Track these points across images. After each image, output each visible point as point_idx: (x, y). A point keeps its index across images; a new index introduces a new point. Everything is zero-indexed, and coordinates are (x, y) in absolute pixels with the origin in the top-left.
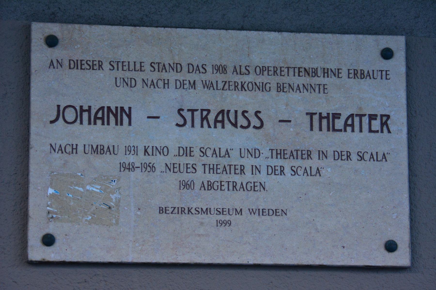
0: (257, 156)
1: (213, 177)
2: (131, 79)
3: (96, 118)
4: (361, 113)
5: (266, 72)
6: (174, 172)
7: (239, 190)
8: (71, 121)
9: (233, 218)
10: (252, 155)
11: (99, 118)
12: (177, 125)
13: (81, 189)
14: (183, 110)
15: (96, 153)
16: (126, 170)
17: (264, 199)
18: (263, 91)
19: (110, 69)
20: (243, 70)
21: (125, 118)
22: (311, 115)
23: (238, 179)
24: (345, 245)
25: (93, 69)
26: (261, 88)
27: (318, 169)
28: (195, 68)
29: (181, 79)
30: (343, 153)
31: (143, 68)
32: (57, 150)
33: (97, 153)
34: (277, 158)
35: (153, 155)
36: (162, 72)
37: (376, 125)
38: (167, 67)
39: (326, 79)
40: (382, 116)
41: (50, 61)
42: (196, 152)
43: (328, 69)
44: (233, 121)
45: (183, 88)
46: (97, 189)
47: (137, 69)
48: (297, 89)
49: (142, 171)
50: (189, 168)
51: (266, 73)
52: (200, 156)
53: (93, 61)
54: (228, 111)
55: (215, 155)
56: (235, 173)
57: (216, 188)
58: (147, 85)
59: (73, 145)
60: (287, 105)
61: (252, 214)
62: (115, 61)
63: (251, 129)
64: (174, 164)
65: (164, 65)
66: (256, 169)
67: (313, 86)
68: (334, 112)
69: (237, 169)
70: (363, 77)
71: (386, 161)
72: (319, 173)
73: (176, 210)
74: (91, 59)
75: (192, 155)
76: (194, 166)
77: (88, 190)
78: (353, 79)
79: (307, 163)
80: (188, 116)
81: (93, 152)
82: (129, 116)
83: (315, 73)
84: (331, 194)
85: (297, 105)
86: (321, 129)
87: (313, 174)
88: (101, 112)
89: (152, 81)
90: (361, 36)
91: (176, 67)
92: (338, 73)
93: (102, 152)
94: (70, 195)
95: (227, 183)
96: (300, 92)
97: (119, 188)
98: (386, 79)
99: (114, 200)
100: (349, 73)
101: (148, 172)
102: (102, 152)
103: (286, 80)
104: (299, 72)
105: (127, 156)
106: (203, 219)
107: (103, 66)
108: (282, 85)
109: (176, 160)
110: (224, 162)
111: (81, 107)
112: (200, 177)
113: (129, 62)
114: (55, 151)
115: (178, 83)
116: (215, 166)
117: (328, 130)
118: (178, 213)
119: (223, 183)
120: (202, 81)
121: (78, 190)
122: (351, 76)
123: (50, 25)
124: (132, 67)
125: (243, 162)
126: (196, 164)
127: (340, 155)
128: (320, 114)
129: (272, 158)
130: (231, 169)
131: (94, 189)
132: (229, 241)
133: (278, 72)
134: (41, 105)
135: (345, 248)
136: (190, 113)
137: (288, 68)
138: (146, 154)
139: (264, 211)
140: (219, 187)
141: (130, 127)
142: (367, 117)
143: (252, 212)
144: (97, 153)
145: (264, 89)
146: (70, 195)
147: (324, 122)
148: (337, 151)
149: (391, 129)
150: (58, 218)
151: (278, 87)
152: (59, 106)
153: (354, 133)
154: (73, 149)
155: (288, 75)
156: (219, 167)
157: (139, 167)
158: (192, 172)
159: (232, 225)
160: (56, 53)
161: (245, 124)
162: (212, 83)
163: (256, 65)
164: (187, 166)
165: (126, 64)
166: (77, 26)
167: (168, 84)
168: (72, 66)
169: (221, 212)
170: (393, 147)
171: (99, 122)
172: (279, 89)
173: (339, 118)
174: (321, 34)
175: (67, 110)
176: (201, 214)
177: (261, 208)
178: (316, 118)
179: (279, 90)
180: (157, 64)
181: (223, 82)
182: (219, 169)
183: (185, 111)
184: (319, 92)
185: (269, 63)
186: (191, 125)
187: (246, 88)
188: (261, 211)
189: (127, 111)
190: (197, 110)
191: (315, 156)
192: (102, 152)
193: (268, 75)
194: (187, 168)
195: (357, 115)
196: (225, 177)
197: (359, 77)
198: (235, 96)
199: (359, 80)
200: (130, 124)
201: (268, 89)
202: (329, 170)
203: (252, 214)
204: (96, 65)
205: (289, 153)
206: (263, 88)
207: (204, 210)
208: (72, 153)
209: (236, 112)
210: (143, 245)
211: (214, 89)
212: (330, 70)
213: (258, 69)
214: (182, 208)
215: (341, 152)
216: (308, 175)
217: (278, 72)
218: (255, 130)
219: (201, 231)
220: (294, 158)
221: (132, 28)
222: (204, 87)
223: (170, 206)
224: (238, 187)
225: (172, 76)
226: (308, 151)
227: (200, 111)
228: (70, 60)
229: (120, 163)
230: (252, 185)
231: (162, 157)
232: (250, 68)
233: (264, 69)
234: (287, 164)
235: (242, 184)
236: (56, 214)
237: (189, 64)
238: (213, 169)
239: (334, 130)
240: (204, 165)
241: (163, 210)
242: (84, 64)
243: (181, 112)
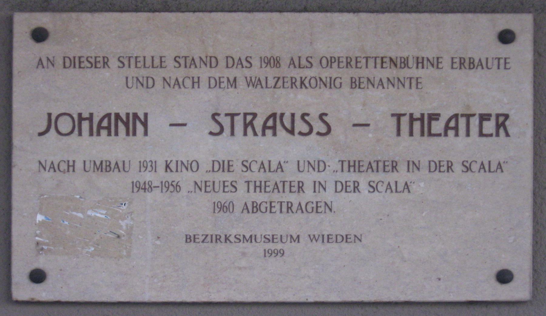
1: (260, 197)
3: (100, 127)
9: (288, 247)
10: (314, 169)
11: (104, 128)
12: (211, 133)
14: (218, 115)
18: (330, 88)
20: (304, 62)
22: (399, 117)
23: (294, 198)
26: (328, 85)
27: (406, 184)
31: (163, 64)
32: (47, 168)
34: (349, 171)
35: (177, 171)
37: (489, 126)
38: (197, 61)
40: (498, 116)
42: (237, 166)
51: (335, 65)
54: (282, 115)
57: (263, 209)
58: (169, 85)
60: (364, 105)
63: (313, 136)
65: (193, 59)
76: (234, 184)
77: (89, 216)
79: (391, 177)
80: (226, 122)
82: (145, 124)
83: (405, 63)
85: (379, 104)
91: (211, 61)
92: (438, 63)
97: (131, 213)
100: (453, 63)
109: (210, 177)
111: (80, 115)
112: (242, 196)
115: (213, 81)
116: (263, 184)
117: (422, 134)
129: (342, 171)
132: (281, 275)
133: (353, 63)
137: (367, 58)
142: (477, 117)
143: (313, 238)
154: (69, 166)
156: (268, 184)
171: (104, 132)
173: (437, 119)
177: (326, 233)
178: (405, 121)
183: (222, 116)
184: (410, 87)
185: (339, 51)
186: (230, 134)
187: (307, 85)
189: (142, 117)
190: (238, 114)
191: (402, 168)
193: (339, 67)
194: (224, 186)
195: (462, 115)
196: (276, 197)
197: (467, 67)
199: (467, 71)
200: (146, 133)
205: (366, 165)
206: (331, 84)
207: (248, 237)
209: (293, 115)
212: (425, 60)
213: (324, 61)
217: (353, 63)
218: (318, 137)
219: (243, 263)
224: (294, 208)
225: (204, 73)
227: (242, 116)
230: (314, 205)
234: (363, 180)
235: (300, 204)
238: (260, 187)
239: (430, 134)
241: (189, 239)
243: (216, 117)
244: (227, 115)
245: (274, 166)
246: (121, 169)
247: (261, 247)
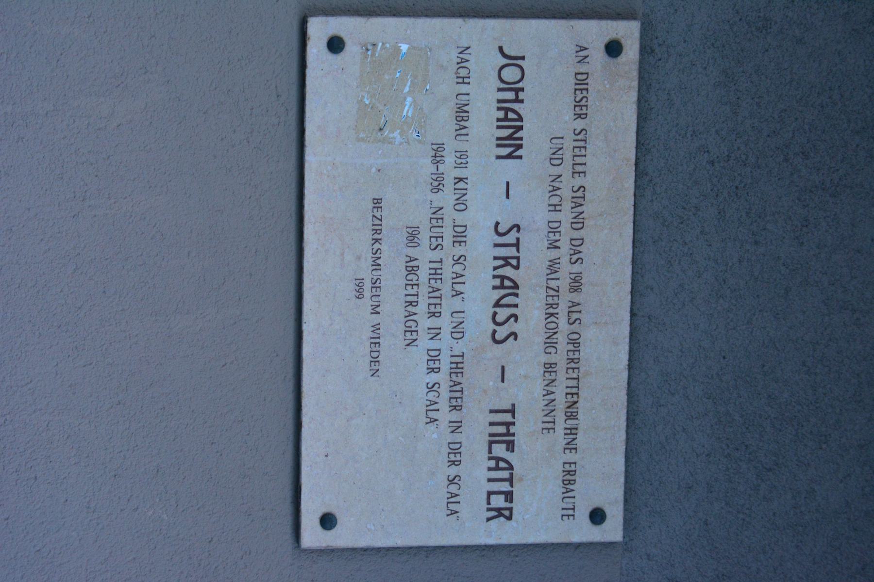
0: (455, 335)
1: (424, 274)
3: (507, 110)
4: (514, 481)
9: (367, 303)
10: (455, 327)
11: (506, 114)
12: (497, 224)
13: (407, 89)
14: (518, 231)
18: (546, 343)
20: (575, 316)
22: (512, 411)
23: (422, 308)
24: (329, 458)
25: (575, 106)
26: (549, 341)
27: (436, 420)
31: (576, 175)
32: (461, 56)
34: (451, 363)
35: (455, 189)
37: (498, 501)
38: (580, 209)
39: (563, 432)
40: (510, 510)
41: (586, 46)
42: (459, 250)
44: (503, 302)
51: (571, 347)
53: (586, 106)
54: (517, 295)
55: (455, 276)
56: (429, 304)
57: (409, 277)
58: (553, 181)
60: (526, 377)
63: (493, 326)
65: (581, 205)
67: (552, 414)
74: (589, 103)
76: (440, 247)
77: (405, 99)
79: (444, 405)
80: (511, 238)
82: (509, 156)
83: (571, 415)
85: (526, 392)
86: (491, 424)
87: (429, 413)
88: (515, 117)
89: (559, 189)
90: (622, 480)
91: (578, 222)
92: (571, 449)
97: (408, 143)
98: (563, 516)
99: (391, 135)
100: (570, 463)
104: (572, 394)
109: (448, 222)
111: (522, 90)
112: (425, 256)
113: (585, 156)
115: (556, 225)
116: (440, 277)
117: (491, 435)
121: (405, 85)
122: (567, 466)
123: (636, 47)
124: (578, 160)
127: (456, 452)
128: (513, 424)
129: (452, 356)
132: (335, 295)
133: (573, 365)
134: (527, 34)
137: (578, 379)
140: (410, 282)
142: (510, 489)
143: (376, 328)
147: (502, 429)
150: (366, 58)
152: (523, 58)
154: (463, 78)
156: (439, 281)
160: (598, 54)
161: (500, 318)
162: (557, 272)
165: (583, 152)
166: (635, 84)
168: (579, 77)
170: (467, 524)
171: (501, 114)
173: (508, 450)
174: (625, 424)
175: (517, 71)
177: (381, 341)
178: (508, 417)
183: (517, 235)
184: (543, 422)
185: (585, 352)
186: (497, 242)
187: (549, 320)
188: (377, 341)
189: (517, 153)
190: (518, 251)
191: (455, 416)
193: (568, 351)
194: (437, 237)
195: (512, 474)
196: (424, 290)
197: (565, 478)
198: (538, 304)
199: (561, 479)
200: (498, 157)
202: (435, 436)
205: (458, 380)
206: (550, 343)
207: (378, 262)
208: (458, 77)
209: (516, 306)
212: (574, 436)
213: (576, 336)
217: (573, 365)
218: (491, 331)
219: (348, 257)
220: (451, 387)
221: (634, 161)
224: (410, 308)
225: (566, 216)
227: (516, 254)
228: (587, 74)
230: (413, 329)
234: (442, 378)
235: (415, 314)
236: (372, 56)
238: (436, 274)
239: (491, 443)
241: (377, 203)
243: (515, 229)
244: (518, 239)
245: (458, 287)
246: (458, 132)
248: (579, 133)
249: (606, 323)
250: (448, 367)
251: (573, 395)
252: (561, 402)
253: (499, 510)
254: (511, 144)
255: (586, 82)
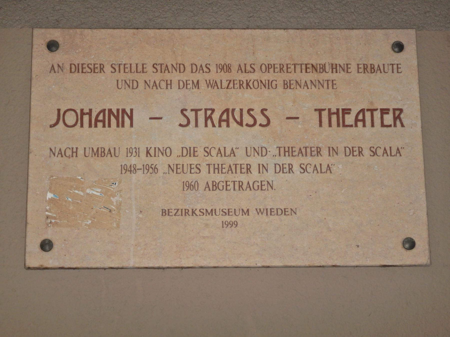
0: (264, 153)
1: (218, 177)
2: (133, 81)
3: (97, 120)
4: (372, 108)
5: (272, 69)
6: (177, 173)
7: (246, 190)
8: (72, 125)
9: (240, 218)
10: (258, 154)
11: (100, 121)
12: (181, 125)
13: (82, 194)
14: (186, 110)
15: (96, 155)
16: (127, 172)
17: (272, 198)
18: (269, 88)
19: (112, 72)
20: (248, 68)
21: (127, 120)
22: (320, 111)
23: (244, 178)
24: (359, 244)
25: (94, 72)
26: (267, 86)
27: (328, 166)
28: (199, 67)
29: (185, 79)
30: (355, 149)
31: (145, 70)
32: (56, 154)
33: (98, 156)
34: (285, 155)
35: (155, 156)
36: (164, 72)
37: (389, 119)
38: (170, 67)
39: (335, 74)
40: (394, 110)
41: (50, 66)
42: (201, 152)
43: (336, 65)
44: (238, 119)
45: (187, 88)
46: (98, 192)
47: (139, 71)
48: (304, 86)
49: (144, 173)
50: (193, 168)
51: (271, 70)
52: (205, 156)
53: (94, 64)
54: (233, 110)
55: (219, 155)
56: (241, 173)
57: (221, 188)
58: (149, 87)
59: (73, 148)
60: (294, 102)
61: (260, 214)
62: (116, 63)
63: (257, 127)
64: (177, 165)
65: (167, 66)
66: (263, 168)
67: (322, 82)
68: (344, 108)
69: (244, 168)
70: (373, 71)
71: (401, 155)
72: (330, 170)
73: (179, 212)
74: (93, 62)
75: (195, 155)
76: (198, 166)
77: (88, 194)
78: (362, 74)
79: (316, 160)
80: (191, 115)
81: (93, 155)
82: (131, 118)
83: (323, 68)
84: (343, 192)
85: (305, 102)
86: (330, 125)
87: (323, 171)
88: (102, 115)
89: (155, 82)
90: (369, 31)
91: (180, 68)
92: (347, 68)
93: (103, 154)
94: (70, 199)
95: (233, 182)
96: (308, 88)
97: (121, 191)
98: (398, 72)
99: (115, 204)
100: (358, 68)
101: (151, 173)
102: (103, 155)
103: (293, 76)
104: (306, 68)
105: (129, 158)
106: (208, 220)
107: (104, 69)
108: (288, 81)
109: (180, 161)
110: (230, 161)
111: (82, 110)
112: (204, 178)
113: (131, 64)
114: (54, 155)
115: (181, 84)
116: (220, 166)
117: (338, 125)
118: (182, 215)
119: (228, 183)
120: (206, 81)
121: (78, 194)
122: (361, 70)
123: (52, 31)
124: (134, 69)
125: (249, 160)
126: (200, 165)
127: (352, 151)
128: (329, 110)
129: (280, 155)
130: (237, 168)
131: (95, 193)
132: (235, 243)
133: (285, 68)
134: (42, 109)
135: (360, 247)
136: (194, 113)
137: (295, 65)
138: (148, 155)
139: (272, 210)
140: (225, 187)
141: (132, 129)
142: (379, 111)
143: (259, 211)
144: (98, 156)
145: (270, 87)
146: (70, 199)
147: (334, 118)
148: (348, 147)
149: (405, 123)
150: (56, 223)
151: (284, 84)
152: (59, 110)
153: (365, 128)
154: (73, 152)
155: (295, 72)
156: (224, 166)
157: (141, 169)
158: (196, 173)
159: (238, 225)
160: (58, 57)
161: (251, 122)
162: (216, 82)
163: (261, 63)
164: (177, 167)
165: (128, 66)
166: (78, 31)
167: (171, 84)
168: (73, 70)
169: (227, 213)
170: (407, 141)
171: (100, 125)
172: (286, 86)
173: (349, 113)
174: (328, 31)
175: (68, 114)
176: (206, 215)
177: (269, 208)
178: (325, 114)
179: (286, 87)
180: (160, 65)
181: (227, 81)
182: (225, 168)
183: (189, 111)
184: (328, 88)
185: (275, 60)
186: (194, 125)
187: (252, 86)
188: (269, 210)
189: (129, 112)
190: (200, 110)
191: (325, 152)
192: (103, 154)
193: (274, 72)
194: (191, 168)
195: (368, 110)
196: (231, 177)
197: (370, 71)
198: (240, 94)
199: (370, 74)
200: (132, 125)
201: (274, 86)
202: (340, 166)
203: (260, 214)
204: (97, 68)
205: (297, 150)
206: (269, 85)
207: (209, 211)
208: (72, 156)
209: (241, 110)
210: (145, 249)
211: (218, 88)
212: (338, 66)
213: (263, 67)
214: (185, 210)
215: (353, 147)
216: (318, 172)
217: (285, 68)
218: (261, 128)
219: (206, 233)
220: (303, 155)
221: (135, 31)
222: (208, 87)
223: (173, 208)
224: (244, 186)
225: (175, 77)
226: (317, 147)
227: (203, 111)
228: (71, 64)
229: (121, 165)
230: (259, 184)
231: (165, 158)
232: (255, 66)
233: (270, 67)
234: (296, 162)
235: (248, 183)
236: (55, 218)
237: (192, 64)
238: (218, 169)
239: (344, 126)
240: (209, 165)
241: (165, 213)
242: (85, 68)
243: (184, 112)
244: (192, 110)
245: (228, 152)
246: (113, 155)
247: (219, 219)
248: (114, 69)
249: (253, 46)
250: (288, 158)
251: (307, 68)
252: (311, 76)
253: (395, 119)
254: (122, 117)
255: (77, 65)
